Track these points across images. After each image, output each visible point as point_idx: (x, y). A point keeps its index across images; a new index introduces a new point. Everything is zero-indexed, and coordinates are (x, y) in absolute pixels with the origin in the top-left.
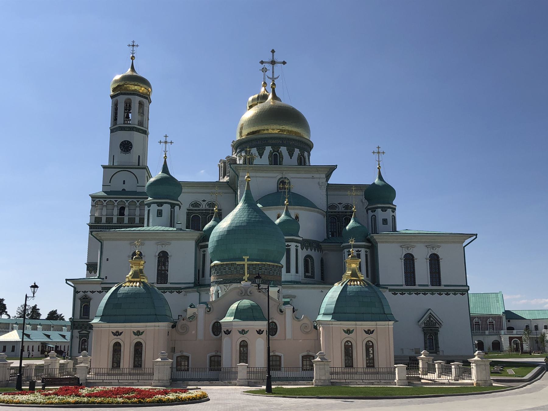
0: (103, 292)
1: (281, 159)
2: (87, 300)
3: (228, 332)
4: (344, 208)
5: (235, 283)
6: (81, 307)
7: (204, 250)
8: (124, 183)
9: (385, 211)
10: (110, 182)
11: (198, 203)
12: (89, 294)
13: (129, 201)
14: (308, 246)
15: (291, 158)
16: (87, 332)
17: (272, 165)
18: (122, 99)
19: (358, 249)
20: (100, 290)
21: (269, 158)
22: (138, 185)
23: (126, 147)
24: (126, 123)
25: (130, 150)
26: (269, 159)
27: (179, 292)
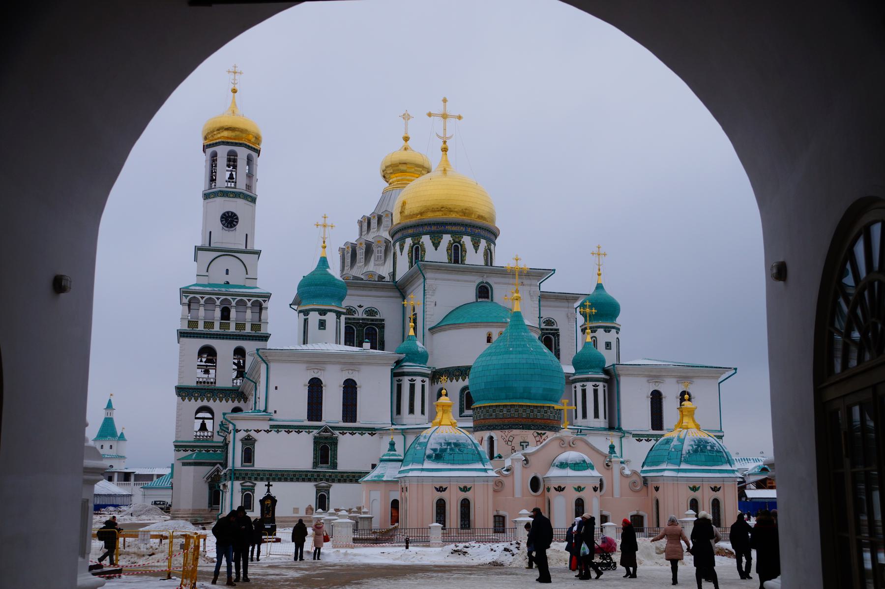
0: (271, 431)
1: (463, 253)
2: (250, 441)
3: (560, 489)
4: (545, 324)
5: (516, 429)
6: (242, 451)
8: (227, 273)
9: (609, 332)
10: (207, 271)
11: (352, 310)
12: (253, 434)
13: (236, 300)
15: (476, 252)
16: (252, 484)
17: (458, 263)
18: (222, 152)
19: (583, 383)
20: (268, 428)
21: (447, 250)
22: (247, 276)
23: (229, 220)
24: (229, 185)
25: (235, 226)
26: (448, 252)
27: (372, 434)
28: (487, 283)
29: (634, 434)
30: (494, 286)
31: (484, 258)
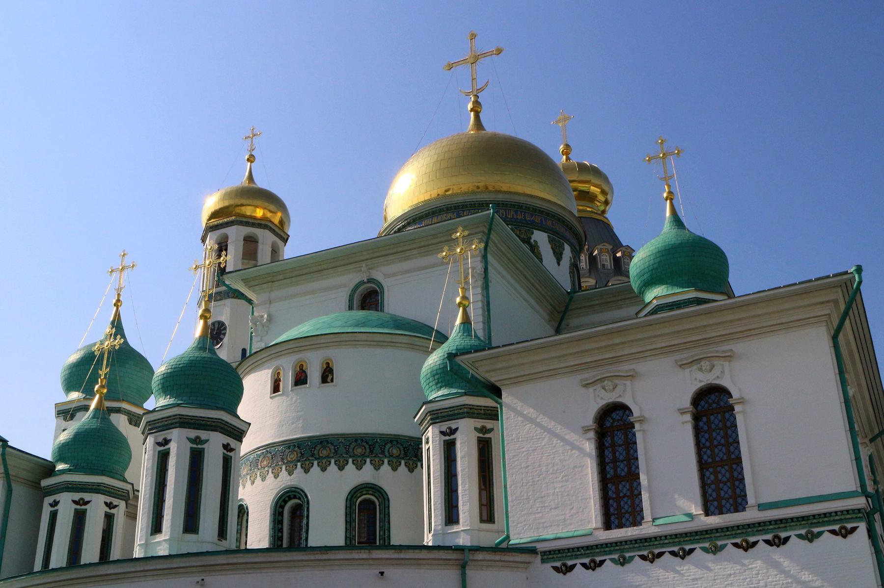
7: (55, 501)
14: (363, 455)
28: (370, 280)
29: (544, 553)
30: (385, 283)
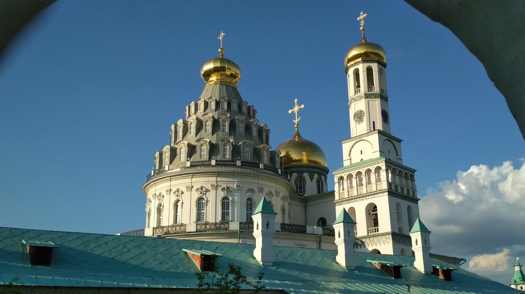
1: (304, 182)
26: (295, 183)
31: (317, 184)
